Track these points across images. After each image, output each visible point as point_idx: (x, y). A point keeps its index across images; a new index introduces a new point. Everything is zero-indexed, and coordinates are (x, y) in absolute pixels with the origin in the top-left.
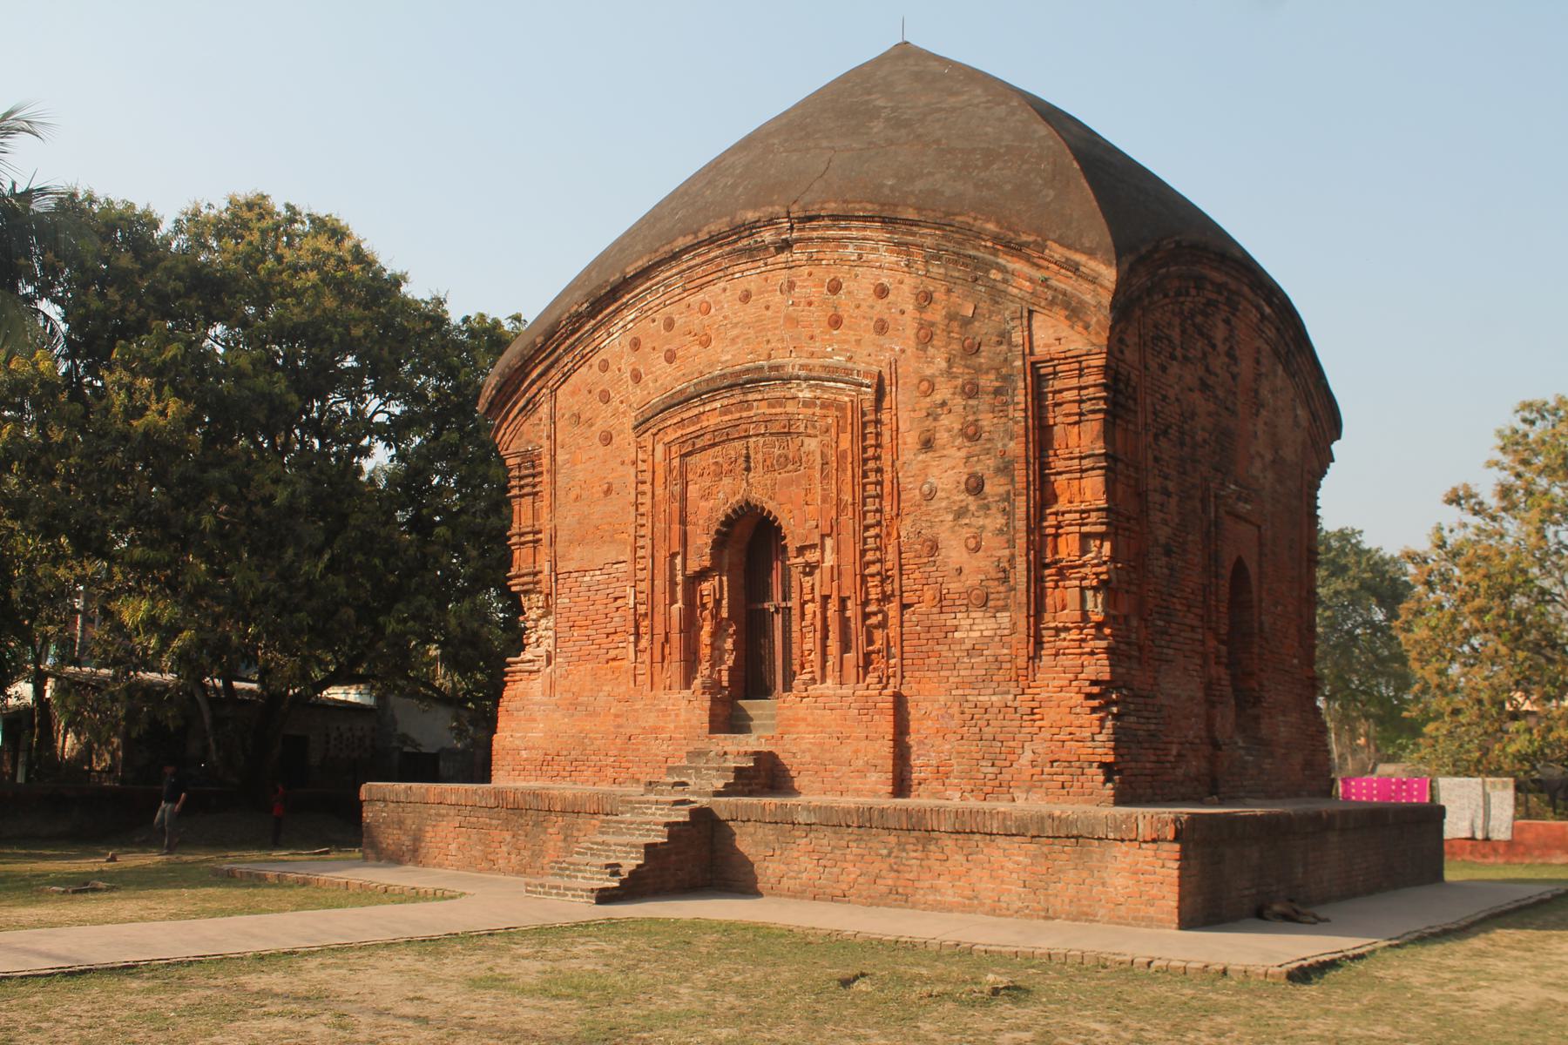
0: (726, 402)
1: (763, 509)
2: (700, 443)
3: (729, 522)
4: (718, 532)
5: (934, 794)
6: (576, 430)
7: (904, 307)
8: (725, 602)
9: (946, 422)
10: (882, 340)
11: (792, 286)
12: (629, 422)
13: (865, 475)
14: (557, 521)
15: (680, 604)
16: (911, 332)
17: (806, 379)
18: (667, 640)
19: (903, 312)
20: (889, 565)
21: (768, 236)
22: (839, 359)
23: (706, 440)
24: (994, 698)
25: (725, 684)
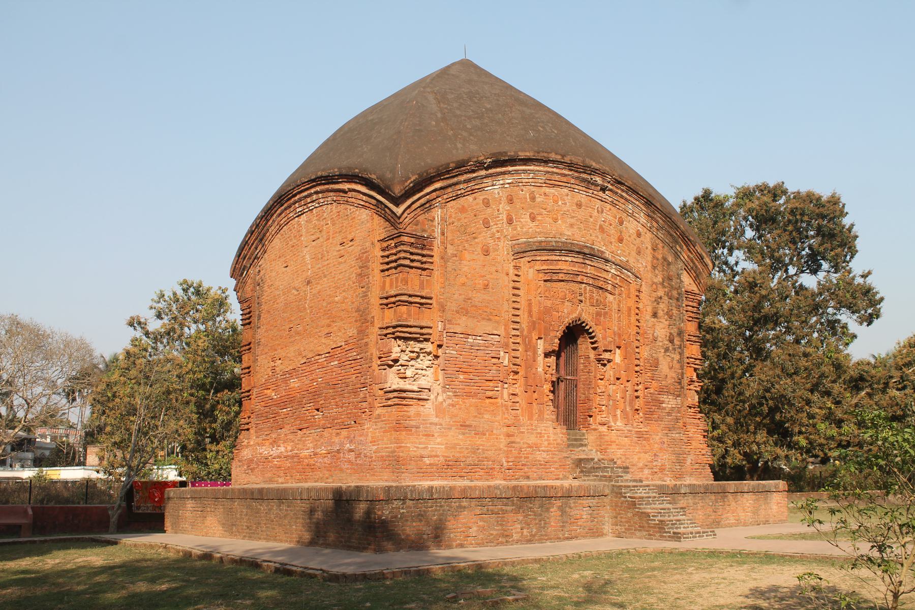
2: (555, 277)
5: (660, 479)
16: (650, 258)
21: (599, 180)
23: (561, 276)
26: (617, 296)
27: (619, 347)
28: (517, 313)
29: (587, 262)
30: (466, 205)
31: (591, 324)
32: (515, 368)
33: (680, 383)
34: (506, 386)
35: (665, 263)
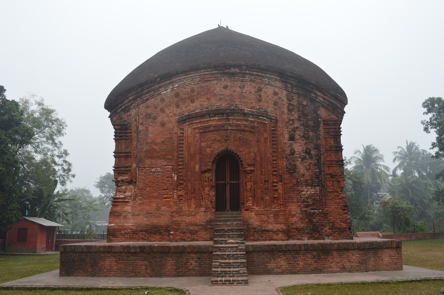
1: (233, 152)
4: (215, 158)
10: (276, 107)
11: (244, 87)
16: (286, 106)
17: (253, 115)
19: (283, 100)
24: (316, 211)
29: (230, 118)
31: (235, 152)
33: (319, 178)
34: (175, 191)
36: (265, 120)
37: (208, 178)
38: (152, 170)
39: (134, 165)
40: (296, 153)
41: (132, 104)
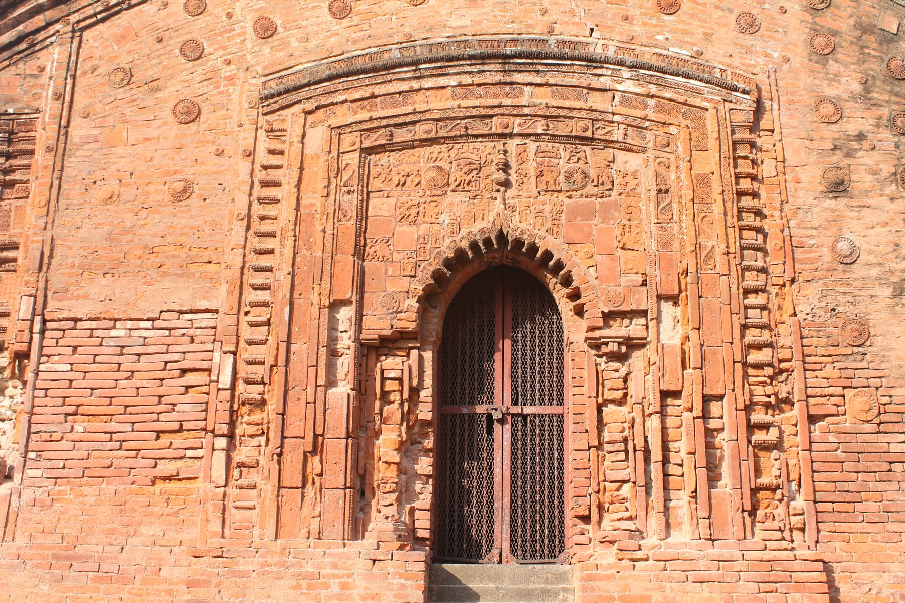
0: (467, 80)
1: (534, 248)
2: (402, 135)
3: (458, 260)
4: (437, 276)
6: (120, 93)
7: (787, 5)
8: (426, 394)
9: (869, 162)
10: (748, 40)
12: (254, 86)
13: (740, 218)
14: (57, 231)
15: (344, 389)
17: (633, 67)
18: (316, 449)
20: (785, 354)
22: (685, 53)
23: (420, 131)
25: (425, 534)
26: (651, 154)
27: (674, 300)
28: (268, 244)
30: (136, 24)
32: (254, 392)
35: (871, 41)
36: (699, 93)
37: (400, 380)
38: (113, 333)
39: (25, 308)
40: (864, 257)
41: (49, 24)
